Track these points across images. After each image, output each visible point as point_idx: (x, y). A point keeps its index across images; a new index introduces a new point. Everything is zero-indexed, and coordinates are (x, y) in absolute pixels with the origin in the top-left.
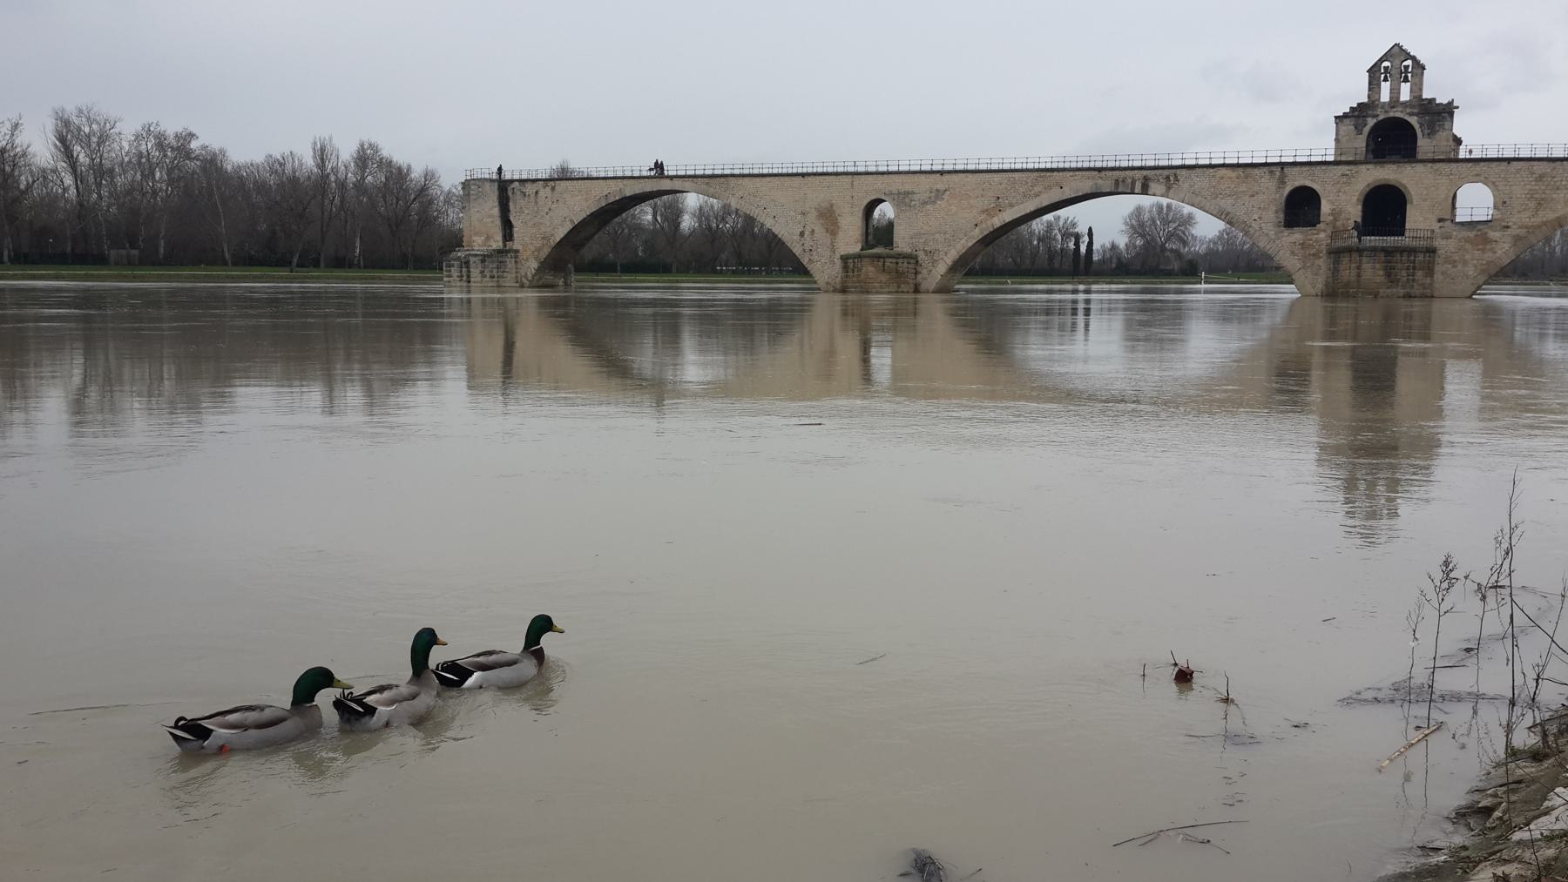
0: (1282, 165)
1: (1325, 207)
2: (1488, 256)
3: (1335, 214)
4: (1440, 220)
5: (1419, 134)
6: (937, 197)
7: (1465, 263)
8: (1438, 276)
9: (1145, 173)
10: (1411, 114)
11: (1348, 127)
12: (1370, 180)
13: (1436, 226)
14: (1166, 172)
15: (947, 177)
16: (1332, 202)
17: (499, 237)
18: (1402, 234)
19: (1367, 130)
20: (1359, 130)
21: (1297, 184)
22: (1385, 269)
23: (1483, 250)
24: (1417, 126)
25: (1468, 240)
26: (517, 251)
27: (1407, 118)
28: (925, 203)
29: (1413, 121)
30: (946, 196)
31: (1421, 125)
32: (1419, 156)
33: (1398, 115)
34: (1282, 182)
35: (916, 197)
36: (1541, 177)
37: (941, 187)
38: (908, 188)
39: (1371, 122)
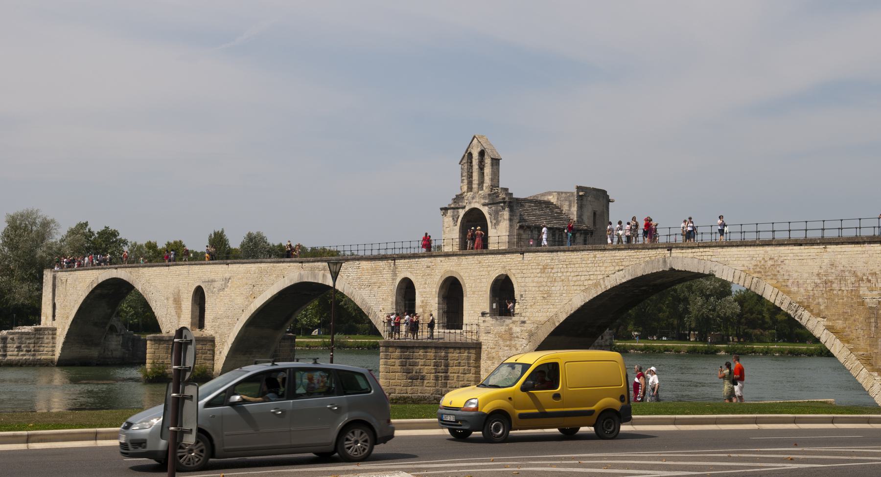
0: (394, 258)
3: (424, 306)
4: (483, 314)
6: (226, 286)
10: (484, 205)
11: (448, 220)
12: (442, 271)
17: (51, 318)
22: (403, 365)
24: (487, 216)
26: (54, 330)
28: (219, 290)
29: (485, 210)
31: (490, 214)
32: (492, 247)
34: (395, 274)
37: (227, 275)
38: (212, 277)
39: (462, 213)
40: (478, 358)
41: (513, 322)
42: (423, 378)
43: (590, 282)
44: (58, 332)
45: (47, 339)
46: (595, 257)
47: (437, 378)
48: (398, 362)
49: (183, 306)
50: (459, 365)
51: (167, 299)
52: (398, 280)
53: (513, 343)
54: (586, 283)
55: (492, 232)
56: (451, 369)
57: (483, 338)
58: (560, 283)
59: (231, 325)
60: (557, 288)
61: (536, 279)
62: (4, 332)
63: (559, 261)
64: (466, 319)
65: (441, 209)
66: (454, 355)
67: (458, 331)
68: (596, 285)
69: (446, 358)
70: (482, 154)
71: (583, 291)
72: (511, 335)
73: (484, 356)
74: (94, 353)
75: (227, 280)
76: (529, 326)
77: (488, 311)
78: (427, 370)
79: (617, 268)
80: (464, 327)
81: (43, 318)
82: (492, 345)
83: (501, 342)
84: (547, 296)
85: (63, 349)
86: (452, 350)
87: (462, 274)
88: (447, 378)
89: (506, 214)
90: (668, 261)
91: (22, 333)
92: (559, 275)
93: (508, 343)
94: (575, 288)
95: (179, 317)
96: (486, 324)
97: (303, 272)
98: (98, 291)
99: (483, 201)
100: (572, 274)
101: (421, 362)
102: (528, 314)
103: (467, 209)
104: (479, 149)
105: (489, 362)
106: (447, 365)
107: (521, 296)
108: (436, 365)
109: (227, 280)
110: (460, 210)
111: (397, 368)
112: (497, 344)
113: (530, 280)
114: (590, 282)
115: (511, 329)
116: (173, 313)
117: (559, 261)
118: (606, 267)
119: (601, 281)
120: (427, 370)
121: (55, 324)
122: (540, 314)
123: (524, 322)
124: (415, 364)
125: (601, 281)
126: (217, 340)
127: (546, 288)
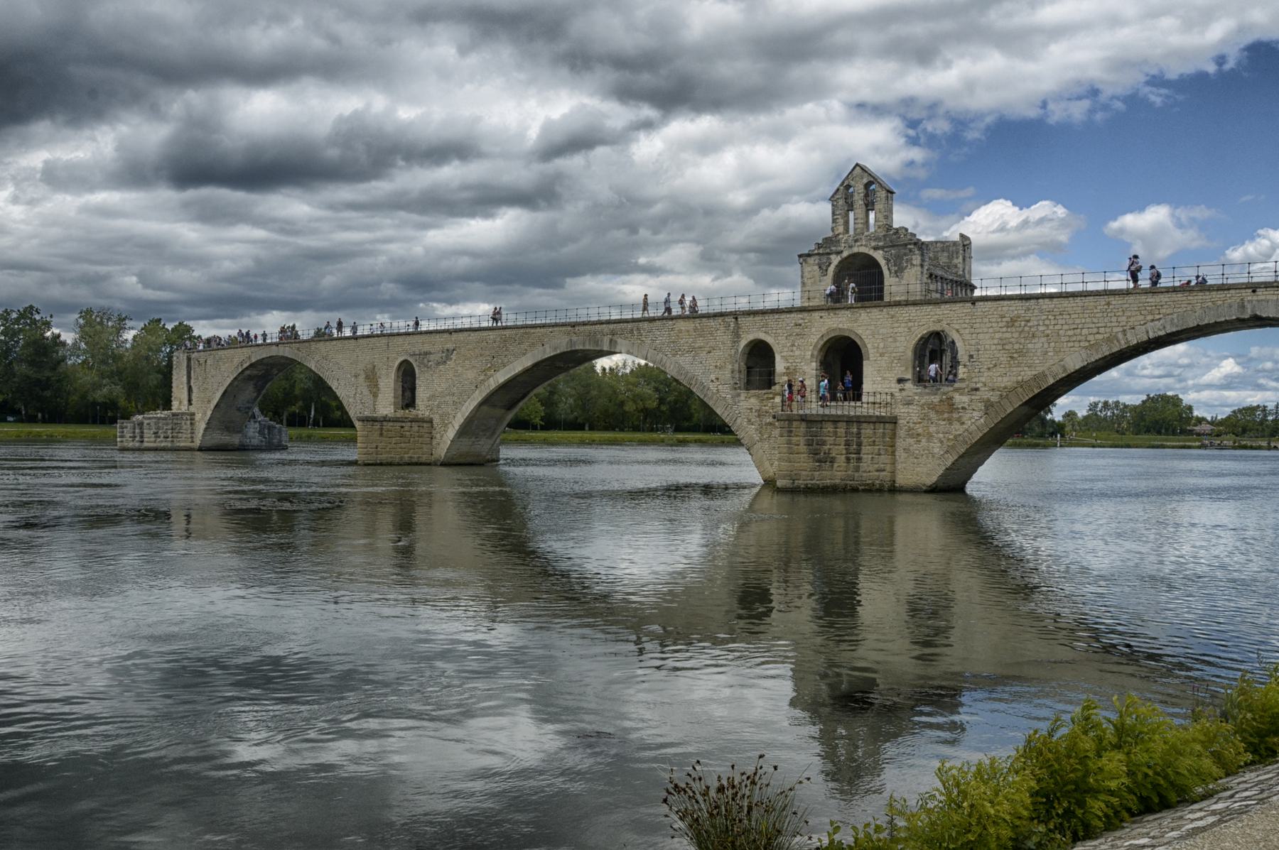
0: (735, 315)
1: (780, 366)
2: (957, 429)
3: (789, 372)
4: (900, 381)
5: (886, 272)
6: (448, 358)
7: (930, 437)
8: (900, 454)
9: (612, 326)
10: (876, 248)
11: (812, 267)
12: (824, 330)
13: (895, 388)
14: (630, 326)
15: (455, 336)
16: (785, 359)
17: (186, 402)
18: (858, 397)
19: (832, 269)
20: (823, 269)
21: (751, 337)
22: (809, 444)
23: (950, 421)
24: (882, 263)
25: (932, 407)
27: (871, 253)
28: (438, 364)
29: (879, 256)
30: (454, 357)
31: (888, 261)
32: (887, 299)
33: (863, 250)
34: (737, 335)
35: (432, 357)
36: (1012, 322)
37: (450, 346)
38: (427, 348)
39: (836, 260)
40: (894, 436)
41: (957, 390)
42: (833, 461)
43: (1100, 337)
44: (198, 417)
45: (186, 426)
46: (1108, 304)
47: (848, 459)
48: (802, 440)
49: (381, 384)
50: (874, 443)
51: (356, 376)
52: (743, 343)
53: (955, 415)
54: (1091, 338)
55: (889, 280)
56: (865, 449)
57: (900, 411)
58: (1044, 339)
59: (457, 405)
60: (1037, 345)
61: (997, 335)
62: (140, 417)
63: (1041, 311)
64: (867, 386)
65: (800, 256)
66: (867, 430)
67: (859, 404)
68: (1109, 340)
69: (859, 433)
70: (867, 186)
71: (1086, 348)
72: (951, 406)
73: (901, 433)
74: (236, 440)
75: (449, 352)
76: (985, 394)
77: (909, 376)
78: (838, 452)
79: (1150, 317)
80: (864, 399)
81: (175, 404)
82: (915, 419)
83: (933, 415)
84: (1017, 355)
85: (204, 435)
86: (865, 425)
87: (859, 332)
88: (859, 459)
89: (917, 260)
90: (1249, 307)
91: (159, 419)
92: (1041, 328)
93: (946, 415)
94: (1070, 344)
95: (375, 396)
96: (904, 393)
97: (574, 338)
98: (248, 372)
99: (873, 244)
100: (1066, 327)
101: (830, 440)
102: (983, 379)
103: (845, 254)
104: (865, 181)
105: (912, 441)
106: (859, 444)
107: (971, 356)
108: (847, 444)
109: (449, 352)
110: (833, 257)
111: (803, 448)
112: (925, 417)
113: (987, 336)
114: (1100, 337)
115: (951, 398)
116: (366, 392)
117: (1041, 311)
118: (1129, 317)
119: (1120, 336)
120: (838, 452)
121: (192, 409)
122: (1005, 379)
123: (977, 389)
124: (824, 443)
125: (1120, 336)
126: (436, 420)
127: (1016, 346)
